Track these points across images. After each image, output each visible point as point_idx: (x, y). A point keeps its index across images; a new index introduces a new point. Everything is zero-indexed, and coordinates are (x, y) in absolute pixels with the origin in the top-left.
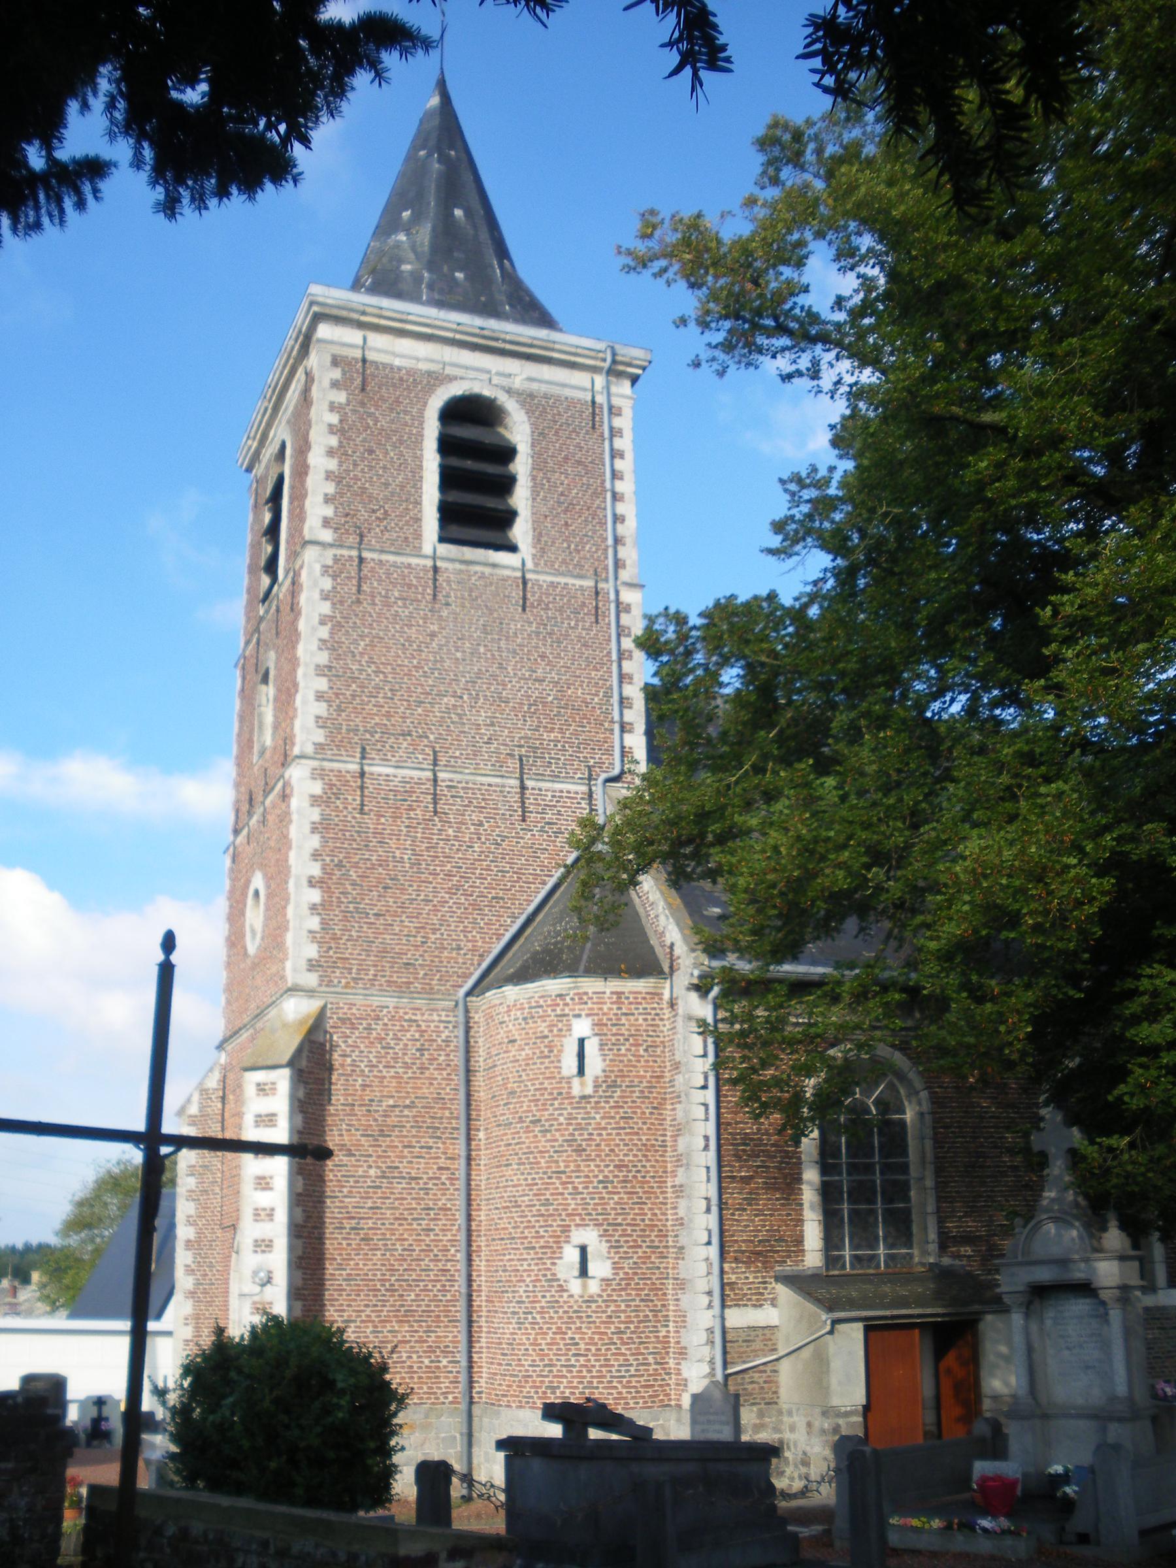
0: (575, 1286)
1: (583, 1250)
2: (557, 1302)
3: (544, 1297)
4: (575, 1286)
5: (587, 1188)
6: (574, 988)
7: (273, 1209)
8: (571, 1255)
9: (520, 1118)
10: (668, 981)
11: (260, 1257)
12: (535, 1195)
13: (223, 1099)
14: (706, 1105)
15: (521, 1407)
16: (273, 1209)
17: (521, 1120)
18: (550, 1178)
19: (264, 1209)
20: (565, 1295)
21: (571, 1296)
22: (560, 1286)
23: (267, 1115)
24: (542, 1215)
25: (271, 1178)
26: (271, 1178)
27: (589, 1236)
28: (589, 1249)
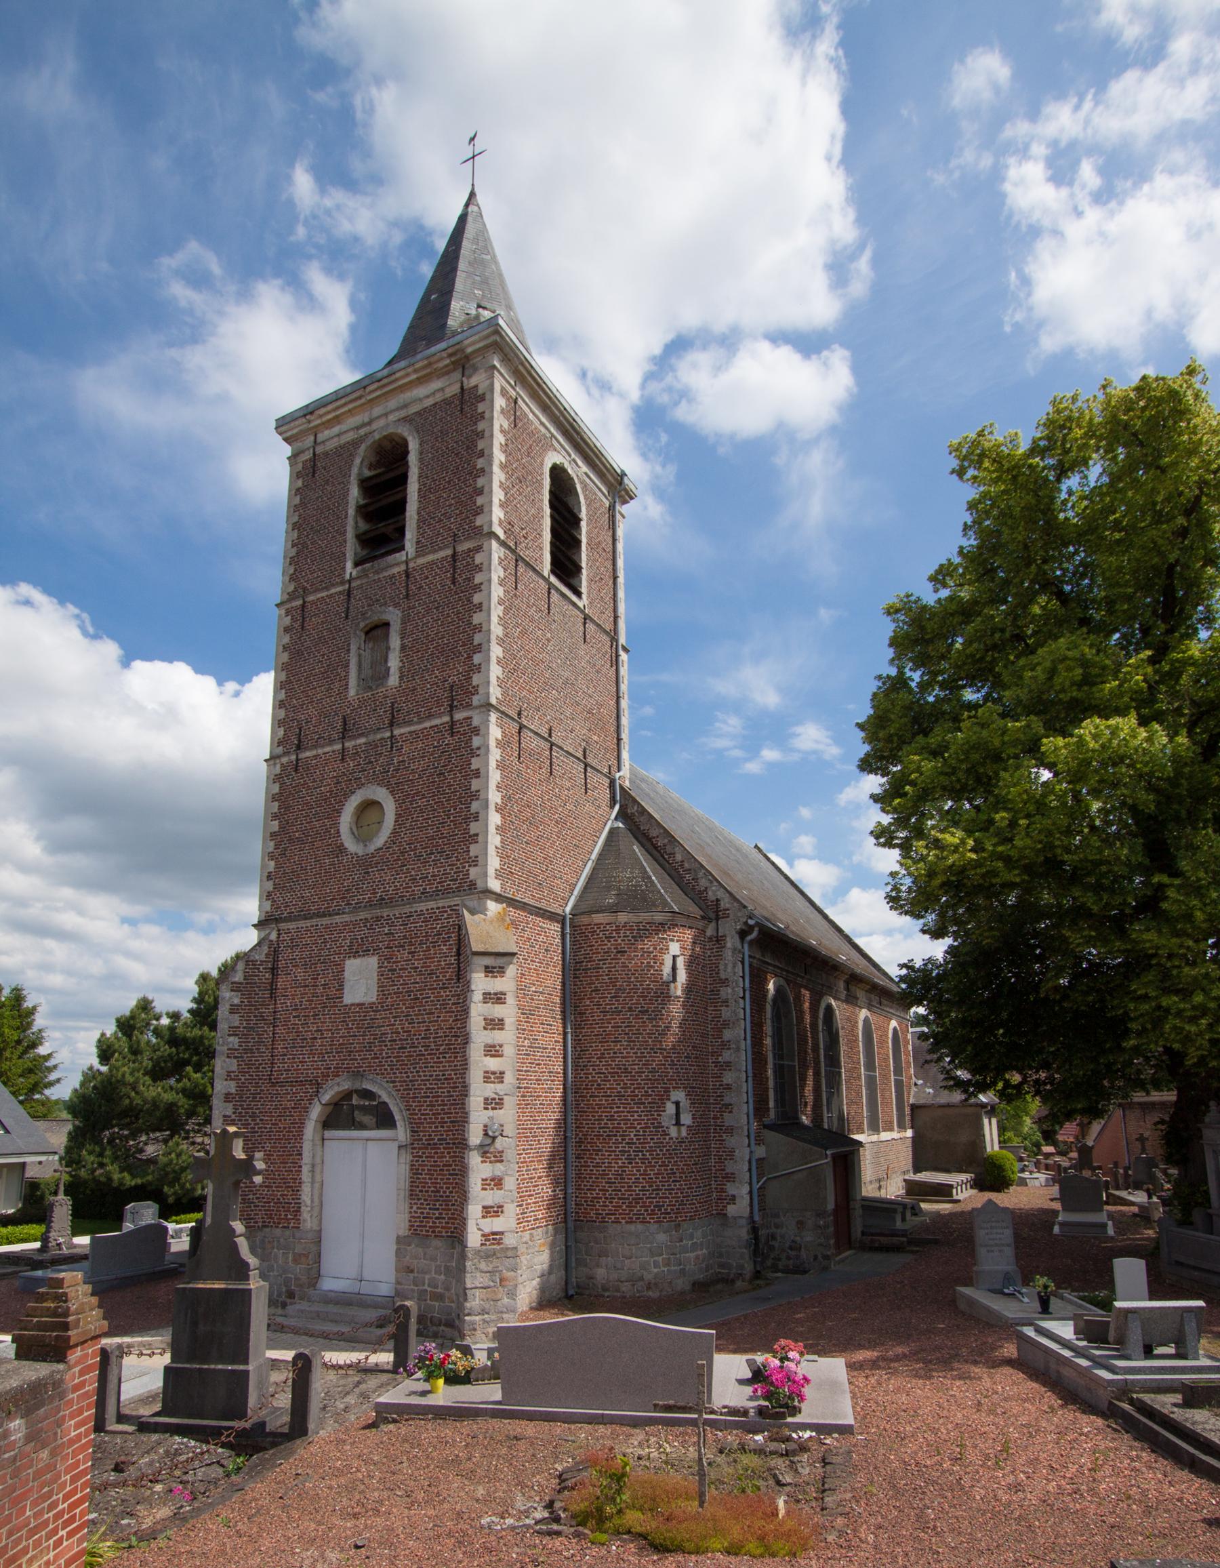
0: (673, 1132)
1: (677, 1104)
2: (662, 1143)
3: (652, 1139)
4: (673, 1132)
5: (678, 1061)
6: (672, 920)
7: (502, 1073)
8: (670, 1108)
9: (631, 1008)
10: (713, 924)
11: (490, 1113)
12: (644, 1065)
13: (274, 970)
15: (631, 1222)
16: (502, 1073)
17: (630, 1009)
18: (655, 1053)
19: (493, 1073)
21: (672, 1138)
22: (663, 1131)
23: (496, 994)
25: (501, 1046)
26: (501, 1046)
27: (679, 1095)
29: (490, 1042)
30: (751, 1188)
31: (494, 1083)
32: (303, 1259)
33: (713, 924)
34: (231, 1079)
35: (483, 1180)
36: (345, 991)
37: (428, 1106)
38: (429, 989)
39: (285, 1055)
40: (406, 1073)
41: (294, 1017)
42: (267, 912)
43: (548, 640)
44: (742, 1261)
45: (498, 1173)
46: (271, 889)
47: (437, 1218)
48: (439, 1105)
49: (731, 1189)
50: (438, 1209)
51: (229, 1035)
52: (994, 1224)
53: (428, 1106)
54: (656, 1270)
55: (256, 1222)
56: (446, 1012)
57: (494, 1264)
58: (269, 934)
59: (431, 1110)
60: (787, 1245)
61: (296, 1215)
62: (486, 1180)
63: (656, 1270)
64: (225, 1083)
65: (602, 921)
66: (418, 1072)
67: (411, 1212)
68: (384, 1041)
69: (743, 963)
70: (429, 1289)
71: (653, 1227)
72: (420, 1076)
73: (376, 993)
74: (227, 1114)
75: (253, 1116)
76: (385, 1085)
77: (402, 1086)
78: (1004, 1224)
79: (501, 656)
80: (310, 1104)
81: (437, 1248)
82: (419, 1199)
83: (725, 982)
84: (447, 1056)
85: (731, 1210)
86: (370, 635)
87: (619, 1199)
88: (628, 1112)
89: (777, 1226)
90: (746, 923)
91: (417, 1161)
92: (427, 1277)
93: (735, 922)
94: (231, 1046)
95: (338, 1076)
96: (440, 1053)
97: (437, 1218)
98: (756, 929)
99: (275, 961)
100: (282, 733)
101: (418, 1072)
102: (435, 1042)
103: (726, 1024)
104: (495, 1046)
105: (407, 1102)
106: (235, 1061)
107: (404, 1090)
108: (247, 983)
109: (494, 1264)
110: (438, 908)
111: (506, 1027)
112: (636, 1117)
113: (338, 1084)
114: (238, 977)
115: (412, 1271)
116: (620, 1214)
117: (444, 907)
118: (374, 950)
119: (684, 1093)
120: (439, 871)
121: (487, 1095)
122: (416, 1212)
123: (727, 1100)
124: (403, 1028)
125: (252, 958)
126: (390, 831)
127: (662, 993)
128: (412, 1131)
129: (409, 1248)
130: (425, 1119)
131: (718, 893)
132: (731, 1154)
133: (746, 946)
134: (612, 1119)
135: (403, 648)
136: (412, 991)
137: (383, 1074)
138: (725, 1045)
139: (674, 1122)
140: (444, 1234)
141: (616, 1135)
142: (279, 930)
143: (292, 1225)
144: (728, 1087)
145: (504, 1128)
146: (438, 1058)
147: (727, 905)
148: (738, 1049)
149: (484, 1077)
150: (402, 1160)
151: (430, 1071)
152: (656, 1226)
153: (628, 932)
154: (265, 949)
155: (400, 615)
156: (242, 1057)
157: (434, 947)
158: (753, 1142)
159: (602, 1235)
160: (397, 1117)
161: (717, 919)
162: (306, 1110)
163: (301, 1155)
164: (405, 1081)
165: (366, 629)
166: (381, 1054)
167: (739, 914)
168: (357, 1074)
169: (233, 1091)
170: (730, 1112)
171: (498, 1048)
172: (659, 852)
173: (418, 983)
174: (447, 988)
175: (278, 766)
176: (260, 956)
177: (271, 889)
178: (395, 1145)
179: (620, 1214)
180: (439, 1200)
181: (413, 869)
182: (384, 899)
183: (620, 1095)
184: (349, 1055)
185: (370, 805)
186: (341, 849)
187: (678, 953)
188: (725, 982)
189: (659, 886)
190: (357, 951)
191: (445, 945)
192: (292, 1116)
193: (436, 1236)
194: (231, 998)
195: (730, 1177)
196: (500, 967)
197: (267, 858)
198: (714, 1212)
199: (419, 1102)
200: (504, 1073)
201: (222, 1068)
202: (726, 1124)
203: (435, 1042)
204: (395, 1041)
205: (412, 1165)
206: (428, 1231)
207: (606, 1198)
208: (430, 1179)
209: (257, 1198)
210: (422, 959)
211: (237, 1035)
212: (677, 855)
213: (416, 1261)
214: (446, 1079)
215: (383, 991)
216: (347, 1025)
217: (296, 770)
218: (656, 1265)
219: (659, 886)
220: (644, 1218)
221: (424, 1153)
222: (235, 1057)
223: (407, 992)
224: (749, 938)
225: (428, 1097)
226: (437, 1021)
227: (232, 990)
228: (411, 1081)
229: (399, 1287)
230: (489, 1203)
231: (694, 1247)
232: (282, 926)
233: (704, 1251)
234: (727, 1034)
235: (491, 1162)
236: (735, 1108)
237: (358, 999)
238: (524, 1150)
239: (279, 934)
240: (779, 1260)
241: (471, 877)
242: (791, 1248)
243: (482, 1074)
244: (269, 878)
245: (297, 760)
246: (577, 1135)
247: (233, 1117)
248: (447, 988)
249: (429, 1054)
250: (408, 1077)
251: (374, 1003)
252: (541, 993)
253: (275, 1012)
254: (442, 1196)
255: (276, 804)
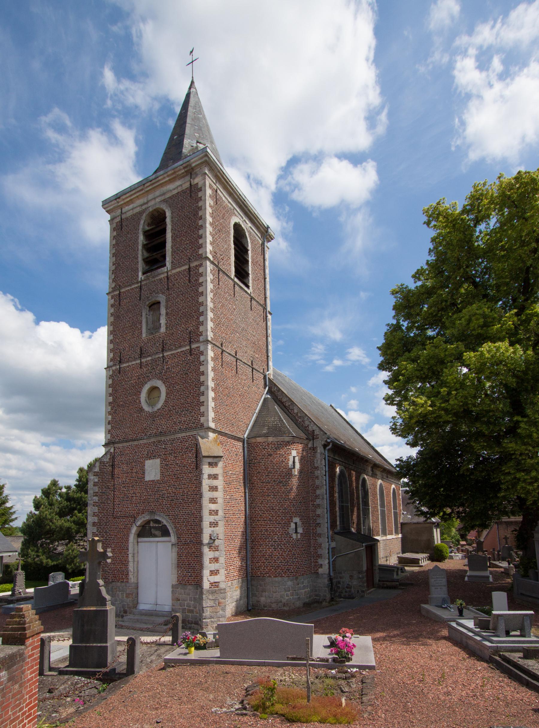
0: (294, 536)
1: (296, 523)
3: (285, 539)
4: (294, 536)
6: (293, 440)
7: (217, 511)
8: (293, 526)
9: (274, 480)
10: (311, 442)
11: (212, 529)
12: (281, 506)
13: (113, 466)
14: (326, 480)
15: (276, 577)
16: (217, 511)
17: (274, 481)
18: (286, 501)
19: (214, 511)
20: (292, 539)
21: (293, 539)
22: (290, 536)
23: (214, 475)
24: (284, 513)
25: (216, 499)
26: (216, 499)
27: (297, 520)
28: (298, 524)
29: (212, 497)
30: (329, 561)
31: (214, 515)
32: (130, 596)
33: (311, 442)
34: (95, 516)
35: (210, 559)
36: (146, 475)
37: (184, 526)
38: (184, 473)
39: (120, 504)
40: (174, 511)
41: (123, 487)
42: (109, 439)
43: (234, 309)
44: (325, 594)
45: (216, 556)
46: (110, 429)
47: (190, 576)
48: (189, 526)
49: (320, 561)
50: (190, 572)
51: (94, 496)
52: (438, 576)
53: (184, 526)
54: (287, 598)
55: (109, 580)
56: (192, 484)
57: (216, 596)
58: (110, 449)
59: (186, 528)
60: (345, 586)
61: (127, 576)
62: (211, 559)
63: (287, 598)
64: (93, 518)
65: (261, 441)
66: (179, 511)
67: (178, 574)
68: (164, 497)
69: (325, 459)
70: (187, 608)
71: (286, 579)
72: (180, 513)
73: (159, 476)
74: (94, 531)
75: (106, 532)
76: (165, 517)
77: (172, 517)
78: (442, 576)
79: (213, 317)
80: (131, 526)
81: (190, 590)
82: (181, 568)
83: (317, 468)
84: (193, 503)
85: (320, 571)
86: (151, 308)
87: (270, 566)
88: (274, 527)
89: (341, 578)
90: (326, 441)
91: (180, 551)
92: (186, 602)
93: (322, 441)
94: (94, 501)
95: (144, 513)
96: (189, 502)
97: (190, 576)
98: (331, 444)
99: (113, 462)
100: (112, 355)
101: (179, 511)
102: (187, 497)
103: (317, 487)
104: (214, 499)
105: (175, 524)
106: (97, 507)
107: (174, 519)
108: (101, 472)
109: (216, 596)
110: (187, 436)
111: (219, 490)
112: (277, 530)
113: (144, 517)
114: (97, 469)
115: (179, 600)
116: (271, 573)
117: (189, 436)
118: (158, 456)
119: (299, 519)
120: (187, 419)
121: (211, 521)
122: (180, 574)
123: (318, 521)
124: (172, 491)
125: (103, 461)
126: (164, 401)
127: (289, 474)
128: (178, 538)
129: (177, 590)
130: (183, 532)
131: (314, 427)
132: (320, 546)
133: (326, 452)
134: (267, 531)
135: (167, 314)
136: (176, 474)
137: (164, 512)
138: (317, 497)
139: (294, 532)
140: (193, 583)
141: (269, 538)
142: (114, 448)
143: (125, 581)
144: (319, 516)
145: (219, 535)
146: (189, 504)
147: (318, 433)
148: (323, 498)
149: (209, 513)
150: (174, 551)
151: (185, 510)
152: (287, 578)
153: (273, 446)
154: (109, 456)
155: (165, 298)
156: (100, 506)
157: (185, 454)
158: (330, 540)
159: (263, 583)
160: (171, 531)
161: (313, 439)
162: (130, 529)
163: (128, 549)
164: (174, 515)
165: (150, 305)
166: (163, 503)
167: (323, 437)
168: (152, 513)
169: (96, 521)
170: (320, 527)
171: (215, 499)
172: (286, 408)
173: (178, 471)
174: (192, 473)
175: (111, 371)
176: (106, 460)
177: (110, 429)
178: (170, 544)
179: (271, 573)
180: (190, 568)
181: (175, 418)
182: (162, 432)
183: (270, 520)
184: (148, 504)
185: (154, 389)
186: (141, 410)
187: (296, 455)
188: (317, 468)
189: (287, 425)
190: (150, 457)
191: (190, 453)
192: (124, 532)
193: (189, 584)
194: (94, 479)
195: (320, 556)
196: (215, 463)
197: (108, 414)
198: (313, 572)
199: (180, 524)
200: (218, 511)
201: (91, 511)
202: (318, 532)
203: (187, 497)
204: (169, 497)
205: (178, 553)
206: (186, 582)
207: (265, 566)
208: (186, 559)
209: (109, 569)
210: (180, 460)
211: (97, 496)
212: (295, 410)
213: (181, 596)
214: (192, 514)
215: (163, 474)
216: (147, 490)
217: (119, 373)
218: (287, 595)
219: (287, 425)
220: (282, 575)
221: (183, 547)
222: (97, 506)
223: (174, 475)
224: (328, 448)
225: (185, 522)
226: (188, 488)
227: (94, 476)
228: (176, 515)
229: (174, 607)
230: (213, 569)
231: (304, 587)
232: (116, 445)
233: (309, 589)
234: (318, 492)
235: (213, 551)
236: (322, 525)
237: (152, 478)
238: (228, 545)
239: (115, 449)
240: (342, 593)
241: (202, 422)
242: (347, 587)
243: (208, 511)
244: (109, 423)
245: (120, 368)
246: (251, 538)
247: (97, 533)
248: (192, 473)
249: (184, 503)
250: (175, 513)
251: (159, 480)
252: (234, 474)
253: (114, 485)
254: (192, 567)
255: (111, 389)
